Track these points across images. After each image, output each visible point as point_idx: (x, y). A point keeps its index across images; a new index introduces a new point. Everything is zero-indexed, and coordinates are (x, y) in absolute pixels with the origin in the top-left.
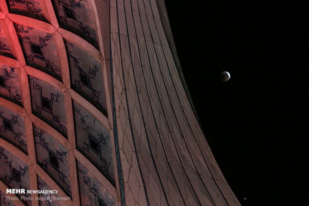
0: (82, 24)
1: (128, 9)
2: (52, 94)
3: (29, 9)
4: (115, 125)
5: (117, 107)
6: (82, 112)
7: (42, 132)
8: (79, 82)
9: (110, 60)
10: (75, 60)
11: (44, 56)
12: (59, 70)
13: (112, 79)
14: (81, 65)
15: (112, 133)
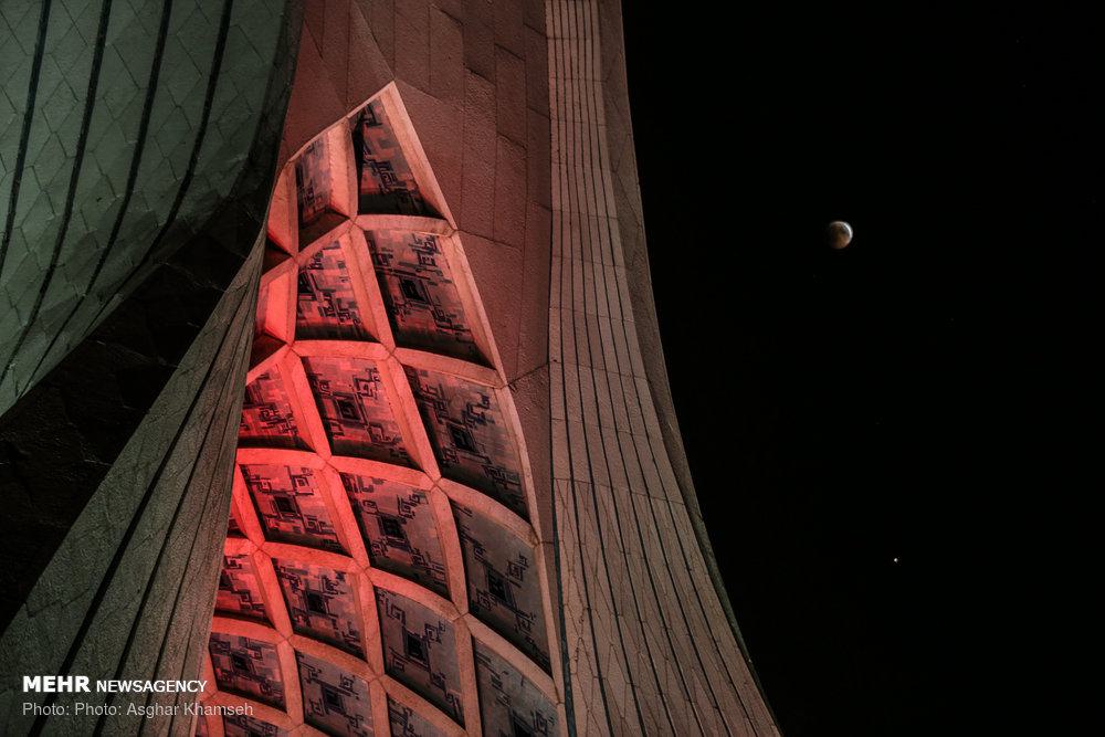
0: (490, 462)
1: (591, 422)
2: (427, 626)
3: (374, 438)
4: (569, 694)
5: (572, 652)
6: (495, 664)
7: (408, 713)
8: (485, 594)
9: (553, 544)
10: (477, 545)
11: (407, 542)
12: (443, 570)
13: (560, 587)
14: (489, 556)
15: (561, 709)
